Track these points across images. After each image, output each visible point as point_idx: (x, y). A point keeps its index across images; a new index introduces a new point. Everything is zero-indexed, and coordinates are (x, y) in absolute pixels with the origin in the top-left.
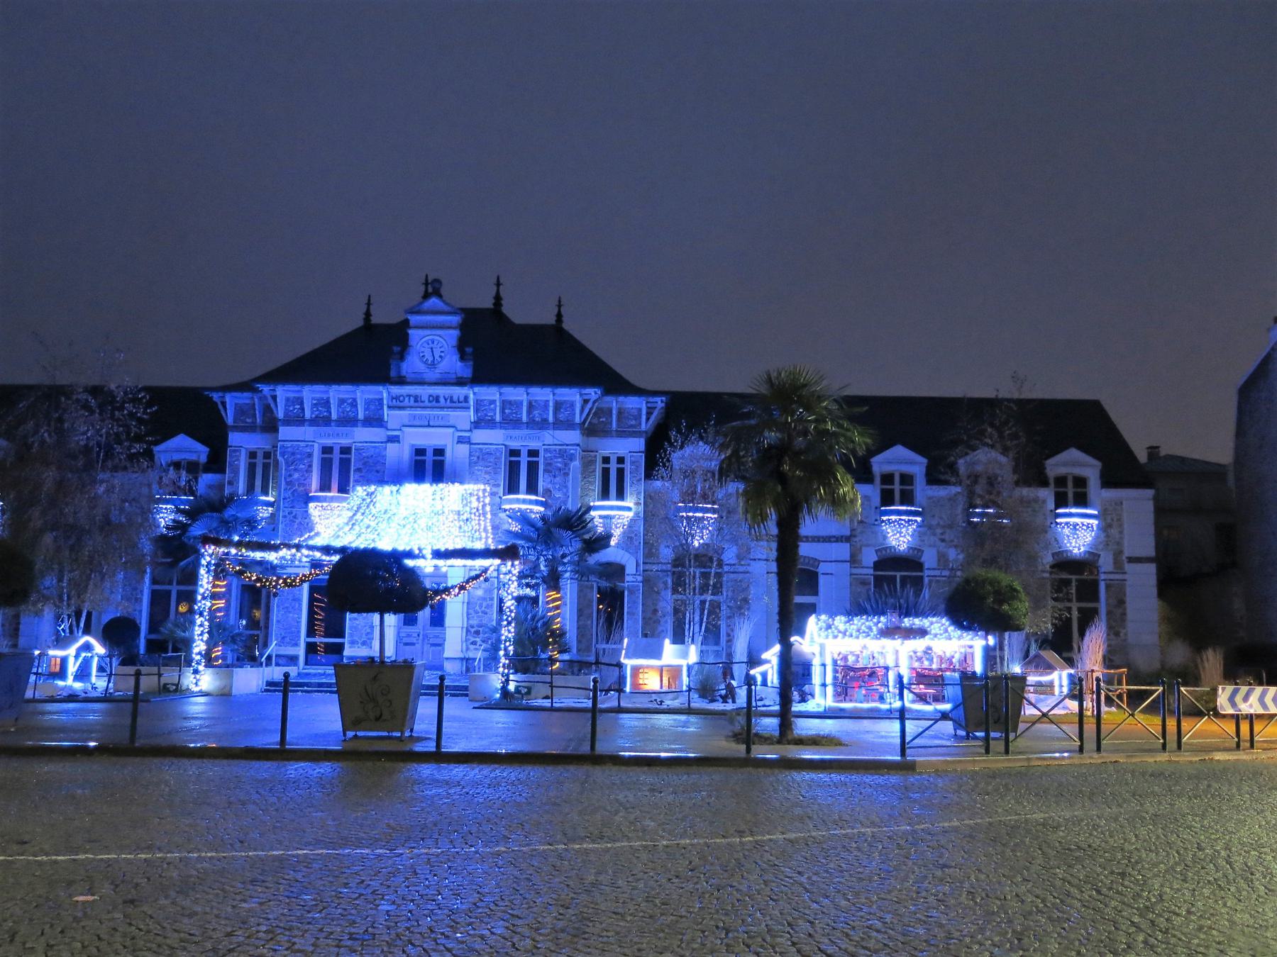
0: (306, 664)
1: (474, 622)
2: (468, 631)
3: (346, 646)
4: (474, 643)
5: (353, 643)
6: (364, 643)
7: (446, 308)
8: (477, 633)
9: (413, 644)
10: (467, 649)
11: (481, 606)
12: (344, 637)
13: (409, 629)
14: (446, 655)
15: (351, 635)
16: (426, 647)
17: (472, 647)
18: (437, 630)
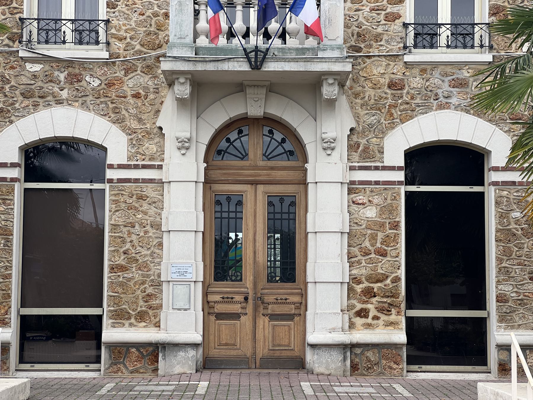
0: (22, 360)
1: (361, 271)
2: (350, 290)
3: (106, 321)
4: (362, 313)
5: (120, 317)
6: (141, 317)
8: (369, 293)
9: (236, 316)
10: (352, 326)
11: (373, 238)
12: (100, 305)
13: (225, 287)
14: (312, 338)
15: (115, 300)
16: (263, 322)
17: (359, 321)
18: (283, 290)
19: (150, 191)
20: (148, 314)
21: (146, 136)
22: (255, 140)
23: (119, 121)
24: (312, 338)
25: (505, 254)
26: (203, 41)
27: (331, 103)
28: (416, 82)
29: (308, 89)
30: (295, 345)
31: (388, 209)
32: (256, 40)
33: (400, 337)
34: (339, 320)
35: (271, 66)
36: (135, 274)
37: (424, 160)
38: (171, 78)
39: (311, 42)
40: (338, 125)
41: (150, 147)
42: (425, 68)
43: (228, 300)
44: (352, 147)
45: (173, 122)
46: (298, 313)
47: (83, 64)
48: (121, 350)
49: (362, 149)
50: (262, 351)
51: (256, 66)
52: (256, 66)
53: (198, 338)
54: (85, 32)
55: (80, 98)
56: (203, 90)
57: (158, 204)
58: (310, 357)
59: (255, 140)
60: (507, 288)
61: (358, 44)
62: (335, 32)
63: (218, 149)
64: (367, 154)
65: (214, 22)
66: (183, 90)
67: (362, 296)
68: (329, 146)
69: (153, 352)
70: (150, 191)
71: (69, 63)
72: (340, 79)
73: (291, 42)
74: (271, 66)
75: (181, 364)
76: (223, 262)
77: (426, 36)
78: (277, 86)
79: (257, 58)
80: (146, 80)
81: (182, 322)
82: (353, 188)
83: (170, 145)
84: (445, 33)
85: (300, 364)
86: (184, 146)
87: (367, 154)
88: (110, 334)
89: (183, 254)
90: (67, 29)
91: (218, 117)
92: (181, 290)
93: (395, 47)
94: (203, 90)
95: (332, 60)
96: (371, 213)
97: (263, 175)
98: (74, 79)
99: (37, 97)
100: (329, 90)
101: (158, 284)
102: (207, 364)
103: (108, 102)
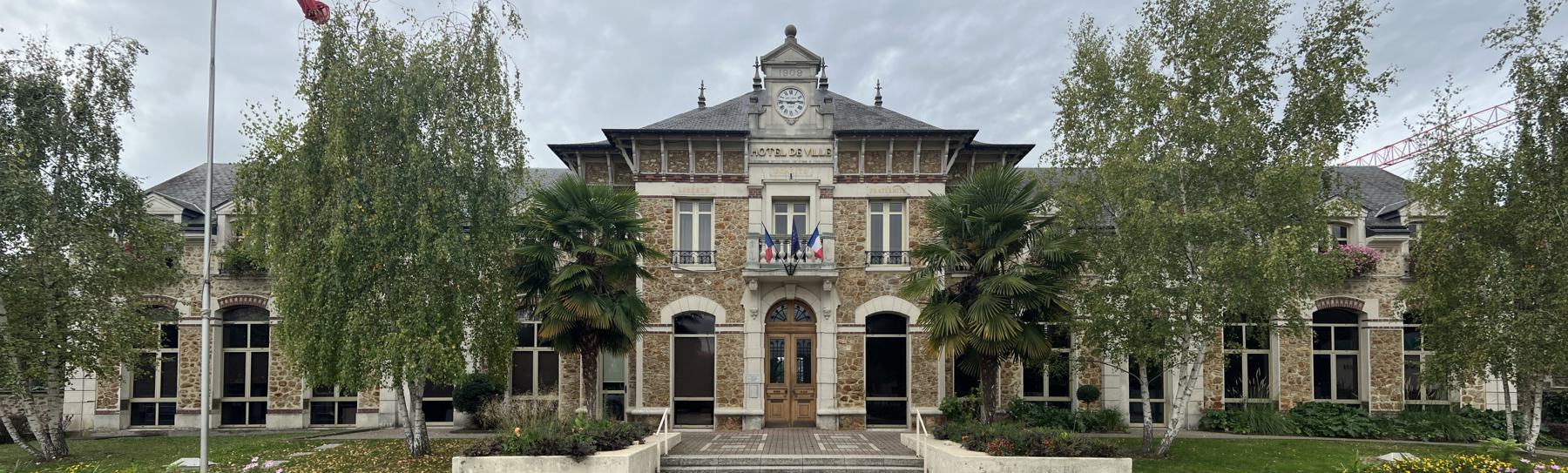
4: (844, 399)
5: (723, 401)
6: (733, 401)
7: (802, 58)
8: (847, 389)
13: (776, 386)
14: (819, 411)
15: (720, 393)
16: (795, 403)
19: (737, 337)
20: (737, 400)
21: (735, 310)
22: (790, 310)
23: (721, 302)
24: (819, 411)
25: (916, 369)
26: (764, 261)
27: (828, 292)
28: (872, 281)
29: (817, 284)
30: (811, 415)
31: (858, 347)
32: (790, 260)
33: (863, 411)
34: (831, 403)
35: (798, 273)
36: (730, 380)
37: (875, 321)
38: (748, 280)
39: (818, 261)
40: (831, 304)
41: (737, 315)
42: (876, 274)
43: (777, 392)
44: (839, 315)
45: (749, 303)
46: (812, 399)
47: (703, 273)
48: (724, 418)
49: (844, 317)
50: (794, 418)
51: (791, 273)
52: (791, 273)
53: (762, 412)
54: (704, 257)
55: (702, 291)
56: (764, 285)
57: (742, 344)
58: (818, 421)
59: (790, 310)
60: (917, 386)
61: (842, 262)
62: (830, 256)
63: (772, 316)
64: (846, 318)
65: (769, 251)
66: (754, 286)
67: (844, 391)
68: (827, 315)
69: (740, 419)
70: (737, 337)
71: (696, 273)
72: (833, 280)
73: (808, 261)
74: (798, 273)
75: (753, 425)
76: (775, 372)
77: (877, 257)
78: (802, 284)
79: (791, 269)
80: (734, 281)
81: (754, 404)
82: (839, 336)
83: (747, 315)
84: (886, 256)
85: (813, 425)
86: (754, 314)
87: (846, 318)
88: (718, 410)
89: (754, 369)
90: (695, 256)
91: (772, 299)
92: (753, 388)
93: (861, 263)
94: (764, 285)
95: (829, 271)
96: (848, 348)
97: (794, 329)
98: (699, 281)
99: (680, 291)
100: (827, 286)
101: (742, 385)
102: (767, 425)
103: (716, 293)
